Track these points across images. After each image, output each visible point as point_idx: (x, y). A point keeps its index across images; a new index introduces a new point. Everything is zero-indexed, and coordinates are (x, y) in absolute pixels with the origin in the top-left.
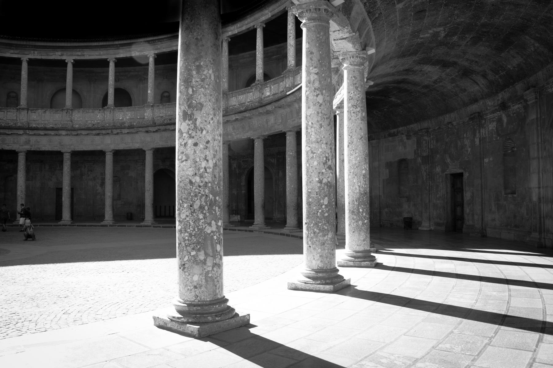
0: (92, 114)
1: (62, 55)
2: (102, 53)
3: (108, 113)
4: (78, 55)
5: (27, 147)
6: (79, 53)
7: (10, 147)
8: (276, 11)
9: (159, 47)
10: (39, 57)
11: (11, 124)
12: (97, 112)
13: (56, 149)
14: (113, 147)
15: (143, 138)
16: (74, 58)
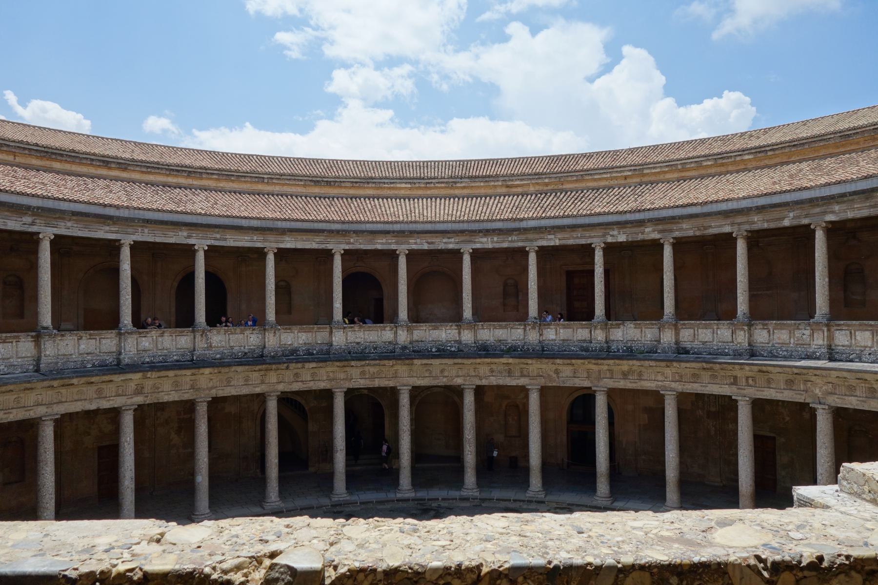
0: (241, 336)
1: (189, 237)
2: (255, 238)
3: (272, 335)
4: (216, 239)
5: (139, 400)
6: (218, 236)
7: (111, 402)
8: (571, 242)
9: (352, 240)
10: (151, 239)
11: (110, 359)
12: (248, 332)
13: (186, 397)
14: (281, 387)
15: (331, 374)
16: (209, 242)
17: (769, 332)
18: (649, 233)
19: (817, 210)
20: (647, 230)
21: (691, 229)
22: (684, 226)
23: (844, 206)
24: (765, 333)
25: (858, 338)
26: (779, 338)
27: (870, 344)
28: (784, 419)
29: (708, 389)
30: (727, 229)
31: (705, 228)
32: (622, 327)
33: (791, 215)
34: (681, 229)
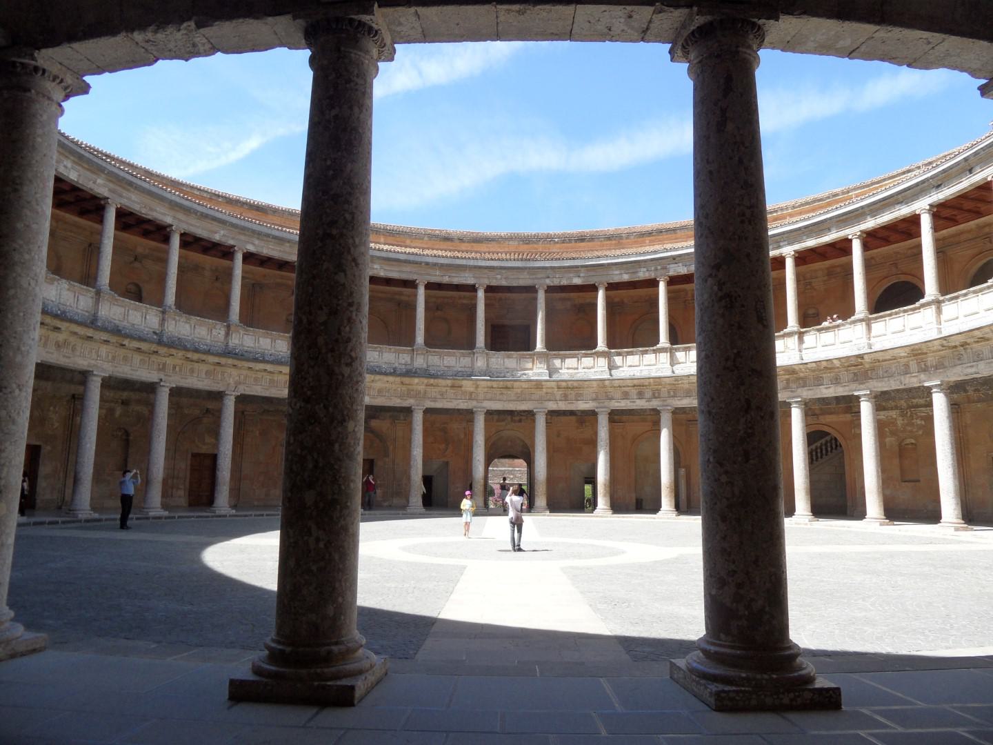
17: (191, 326)
18: (99, 185)
19: (242, 237)
20: (99, 181)
21: (139, 203)
22: (133, 197)
23: (262, 244)
24: (187, 326)
25: (261, 342)
26: (199, 334)
27: (269, 348)
28: (53, 425)
29: (138, 373)
30: (168, 220)
31: (151, 209)
32: (56, 283)
33: (222, 232)
34: (129, 199)
